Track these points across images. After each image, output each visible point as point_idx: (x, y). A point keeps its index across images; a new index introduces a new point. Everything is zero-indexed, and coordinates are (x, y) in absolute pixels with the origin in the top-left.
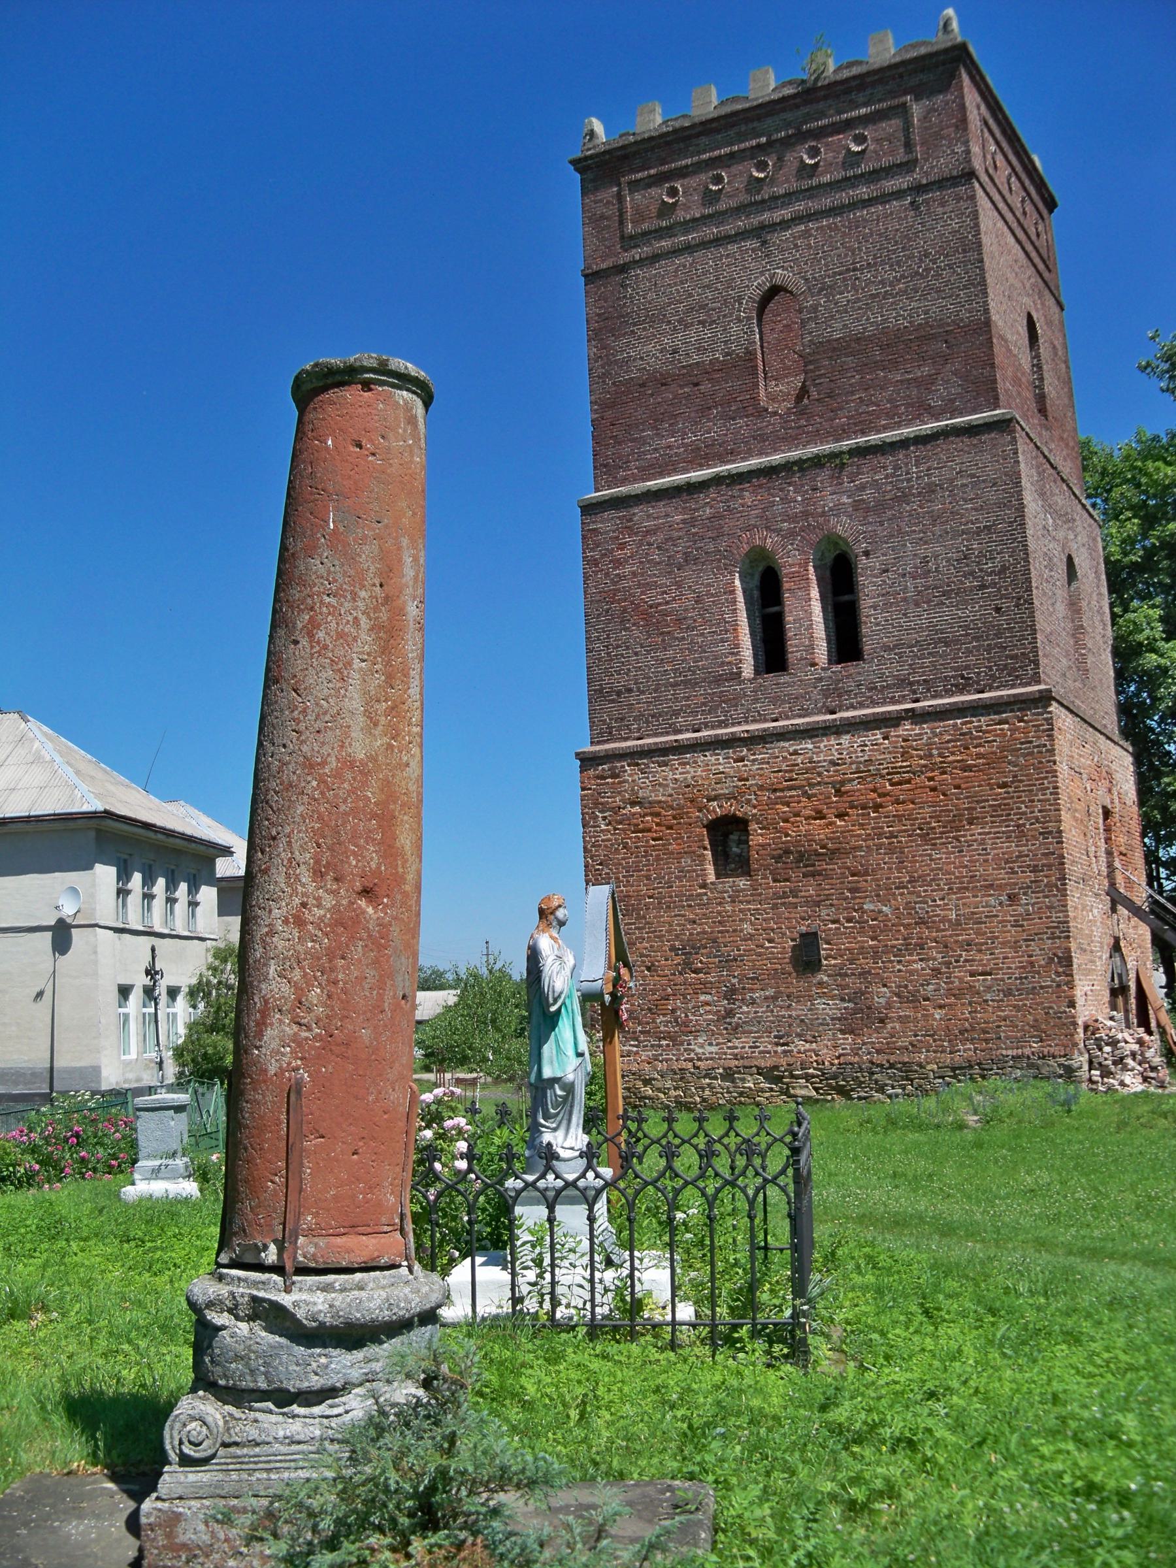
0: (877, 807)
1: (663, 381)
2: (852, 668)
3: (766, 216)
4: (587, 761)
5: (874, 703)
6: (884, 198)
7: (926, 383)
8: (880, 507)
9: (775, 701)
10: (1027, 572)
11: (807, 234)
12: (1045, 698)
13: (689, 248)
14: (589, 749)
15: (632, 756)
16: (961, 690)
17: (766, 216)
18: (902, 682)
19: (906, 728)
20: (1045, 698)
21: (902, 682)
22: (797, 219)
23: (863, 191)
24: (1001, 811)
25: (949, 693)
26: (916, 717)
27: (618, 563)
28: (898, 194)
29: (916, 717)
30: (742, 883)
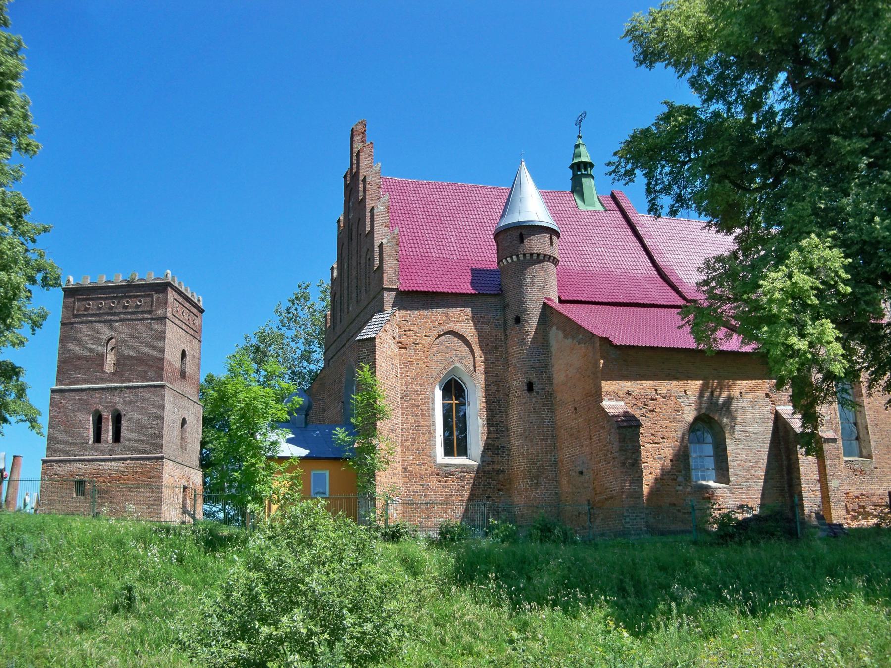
0: (119, 481)
1: (78, 358)
2: (117, 444)
3: (113, 317)
4: (44, 462)
5: (121, 454)
6: (144, 319)
7: (146, 372)
8: (130, 403)
9: (97, 451)
10: (163, 425)
11: (122, 325)
12: (162, 458)
13: (91, 322)
14: (45, 458)
15: (57, 461)
16: (143, 453)
17: (113, 317)
18: (129, 450)
19: (128, 462)
20: (162, 458)
21: (129, 450)
22: (121, 320)
23: (139, 316)
24: (148, 485)
25: (140, 454)
26: (131, 459)
27: (59, 408)
28: (147, 319)
29: (131, 459)
30: (82, 498)
